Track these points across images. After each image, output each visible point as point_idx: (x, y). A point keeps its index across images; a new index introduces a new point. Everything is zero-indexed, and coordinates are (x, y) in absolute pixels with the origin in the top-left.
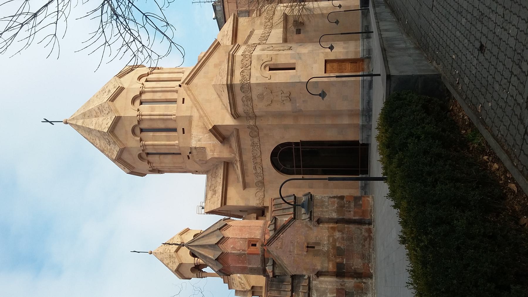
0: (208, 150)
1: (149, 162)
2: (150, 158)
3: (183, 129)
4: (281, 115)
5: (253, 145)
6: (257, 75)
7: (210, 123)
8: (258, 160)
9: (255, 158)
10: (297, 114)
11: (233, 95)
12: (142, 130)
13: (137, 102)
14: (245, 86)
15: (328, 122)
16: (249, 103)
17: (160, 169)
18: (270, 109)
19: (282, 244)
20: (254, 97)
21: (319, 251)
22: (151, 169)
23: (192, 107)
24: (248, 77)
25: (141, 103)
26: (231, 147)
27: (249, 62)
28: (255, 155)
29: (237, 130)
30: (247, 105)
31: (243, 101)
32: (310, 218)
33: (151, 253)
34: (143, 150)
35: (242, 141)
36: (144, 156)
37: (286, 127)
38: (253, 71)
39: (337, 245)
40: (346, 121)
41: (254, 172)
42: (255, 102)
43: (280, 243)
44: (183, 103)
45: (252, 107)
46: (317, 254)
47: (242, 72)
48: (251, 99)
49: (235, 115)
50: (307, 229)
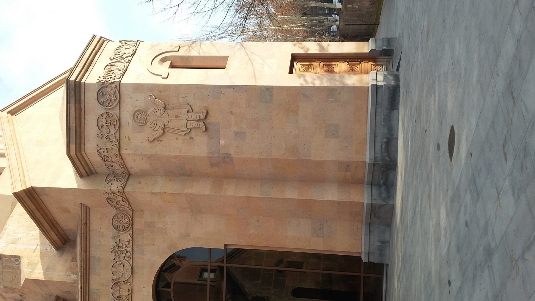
0: (24, 263)
4: (182, 171)
5: (118, 249)
9: (117, 283)
10: (222, 169)
15: (291, 193)
16: (113, 131)
18: (159, 149)
24: (118, 74)
26: (74, 259)
27: (131, 50)
28: (118, 275)
29: (86, 210)
31: (100, 127)
35: (94, 240)
37: (195, 208)
40: (332, 194)
45: (119, 141)
47: (112, 65)
48: (118, 124)
49: (83, 168)
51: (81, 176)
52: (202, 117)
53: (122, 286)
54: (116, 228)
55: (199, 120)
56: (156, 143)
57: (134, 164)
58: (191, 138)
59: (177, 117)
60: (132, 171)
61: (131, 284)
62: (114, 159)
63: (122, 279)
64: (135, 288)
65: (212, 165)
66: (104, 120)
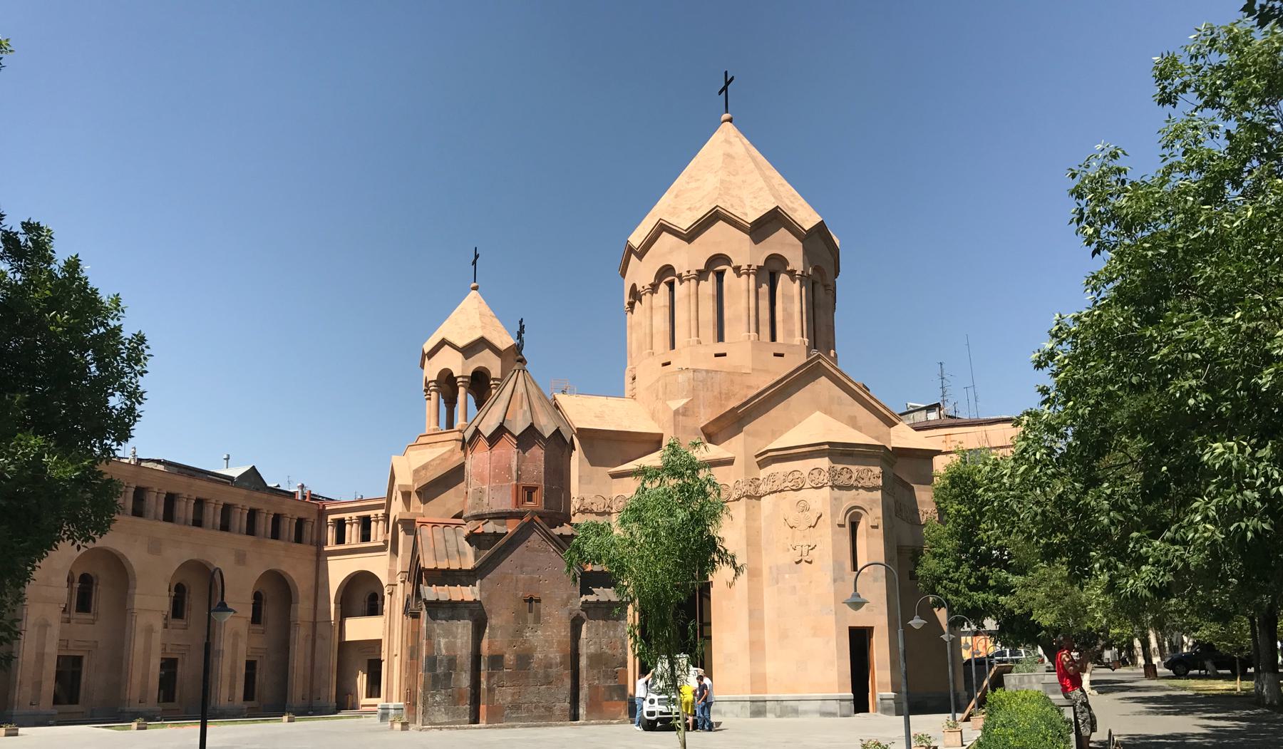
2: (663, 288)
3: (724, 355)
12: (720, 275)
19: (534, 550)
21: (525, 620)
22: (639, 288)
34: (680, 277)
39: (539, 655)
44: (776, 355)
46: (519, 617)
51: (757, 456)
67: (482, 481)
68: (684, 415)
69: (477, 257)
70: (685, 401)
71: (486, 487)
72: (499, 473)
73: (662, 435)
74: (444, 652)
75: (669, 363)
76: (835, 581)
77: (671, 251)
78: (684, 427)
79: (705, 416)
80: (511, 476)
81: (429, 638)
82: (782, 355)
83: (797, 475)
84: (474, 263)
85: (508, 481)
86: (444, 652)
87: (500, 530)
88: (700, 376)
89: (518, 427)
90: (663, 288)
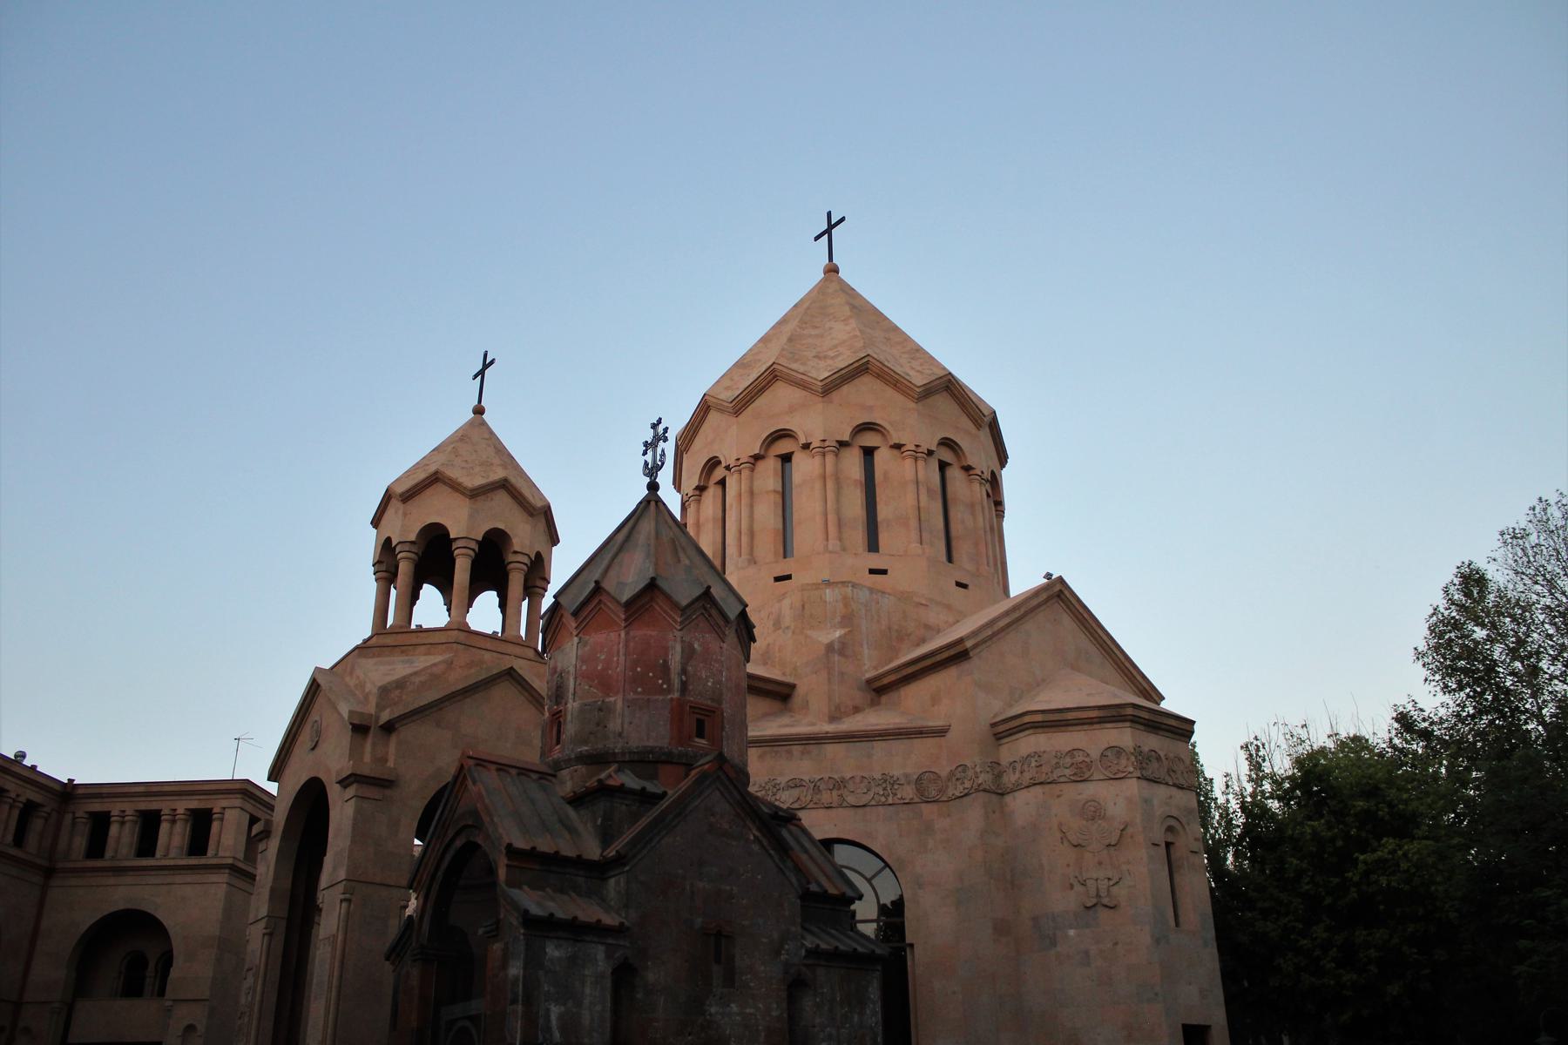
1: (757, 458)
2: (770, 466)
3: (884, 572)
5: (889, 782)
6: (1156, 802)
7: (975, 646)
8: (826, 797)
9: (840, 784)
11: (1090, 722)
12: (869, 452)
13: (947, 456)
14: (1124, 762)
16: (1067, 772)
17: (712, 492)
20: (1089, 790)
23: (949, 607)
25: (943, 466)
26: (857, 710)
28: (851, 786)
30: (1057, 766)
31: (1071, 753)
32: (814, 953)
33: (479, 411)
35: (899, 746)
36: (783, 447)
38: (1161, 792)
41: (783, 780)
42: (1072, 792)
43: (726, 826)
44: (959, 584)
47: (1159, 758)
50: (776, 936)
51: (994, 725)
52: (1105, 901)
53: (835, 793)
54: (919, 779)
55: (1098, 896)
56: (1059, 835)
57: (1023, 805)
58: (1072, 887)
59: (1100, 863)
60: (1008, 798)
61: (840, 806)
62: (1027, 776)
63: (845, 792)
64: (833, 812)
65: (1035, 919)
66: (1080, 759)
67: (606, 686)
68: (842, 653)
69: (486, 365)
70: (838, 634)
71: (617, 701)
72: (648, 674)
73: (793, 687)
74: (557, 1035)
75: (789, 577)
76: (1157, 941)
77: (792, 410)
78: (842, 674)
79: (870, 665)
80: (668, 680)
81: (529, 1001)
82: (964, 586)
83: (1079, 758)
84: (481, 373)
85: (661, 691)
86: (557, 1035)
87: (651, 787)
88: (863, 595)
89: (685, 593)
90: (770, 466)
